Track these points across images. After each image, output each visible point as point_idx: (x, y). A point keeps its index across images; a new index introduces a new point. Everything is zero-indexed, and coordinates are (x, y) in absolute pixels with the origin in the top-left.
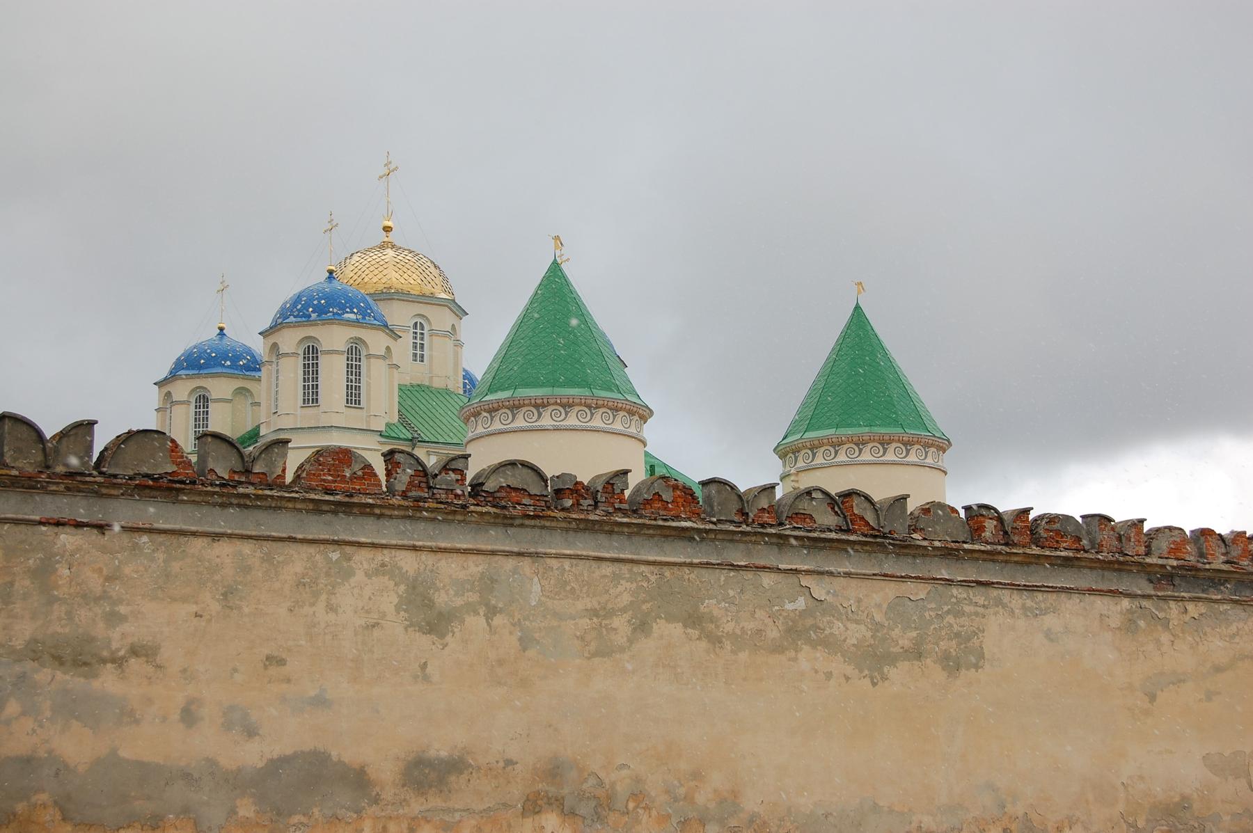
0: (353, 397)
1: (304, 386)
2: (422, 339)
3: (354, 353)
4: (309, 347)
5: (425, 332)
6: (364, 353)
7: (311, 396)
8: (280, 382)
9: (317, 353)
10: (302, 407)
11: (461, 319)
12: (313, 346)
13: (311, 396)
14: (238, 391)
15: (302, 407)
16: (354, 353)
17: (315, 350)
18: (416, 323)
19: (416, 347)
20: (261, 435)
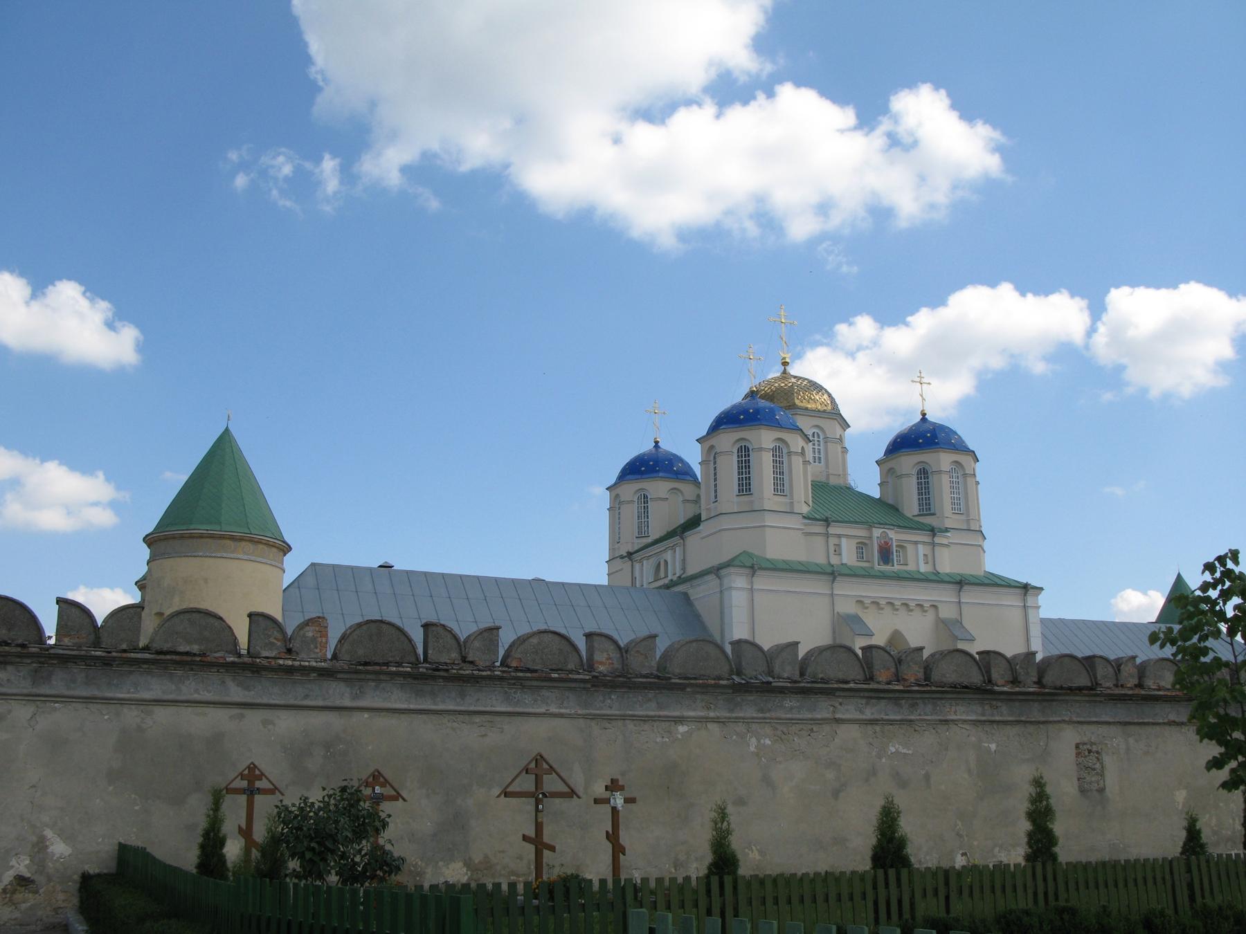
0: (780, 486)
1: (739, 478)
2: (819, 445)
3: (779, 453)
4: (741, 446)
5: (821, 439)
6: (785, 451)
7: (745, 486)
8: (718, 477)
9: (749, 451)
10: (737, 495)
11: (845, 430)
12: (745, 446)
13: (745, 486)
14: (672, 491)
15: (737, 495)
16: (779, 453)
17: (747, 449)
18: (814, 433)
19: (814, 452)
20: (702, 520)
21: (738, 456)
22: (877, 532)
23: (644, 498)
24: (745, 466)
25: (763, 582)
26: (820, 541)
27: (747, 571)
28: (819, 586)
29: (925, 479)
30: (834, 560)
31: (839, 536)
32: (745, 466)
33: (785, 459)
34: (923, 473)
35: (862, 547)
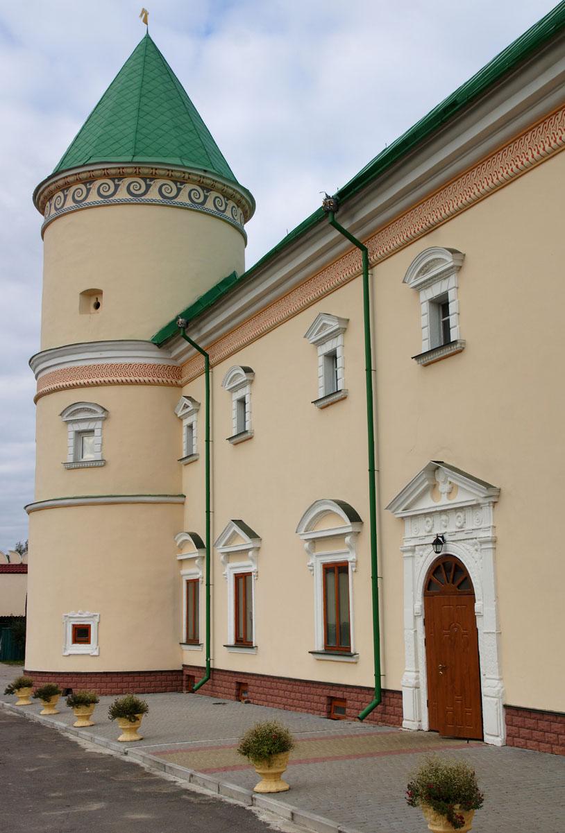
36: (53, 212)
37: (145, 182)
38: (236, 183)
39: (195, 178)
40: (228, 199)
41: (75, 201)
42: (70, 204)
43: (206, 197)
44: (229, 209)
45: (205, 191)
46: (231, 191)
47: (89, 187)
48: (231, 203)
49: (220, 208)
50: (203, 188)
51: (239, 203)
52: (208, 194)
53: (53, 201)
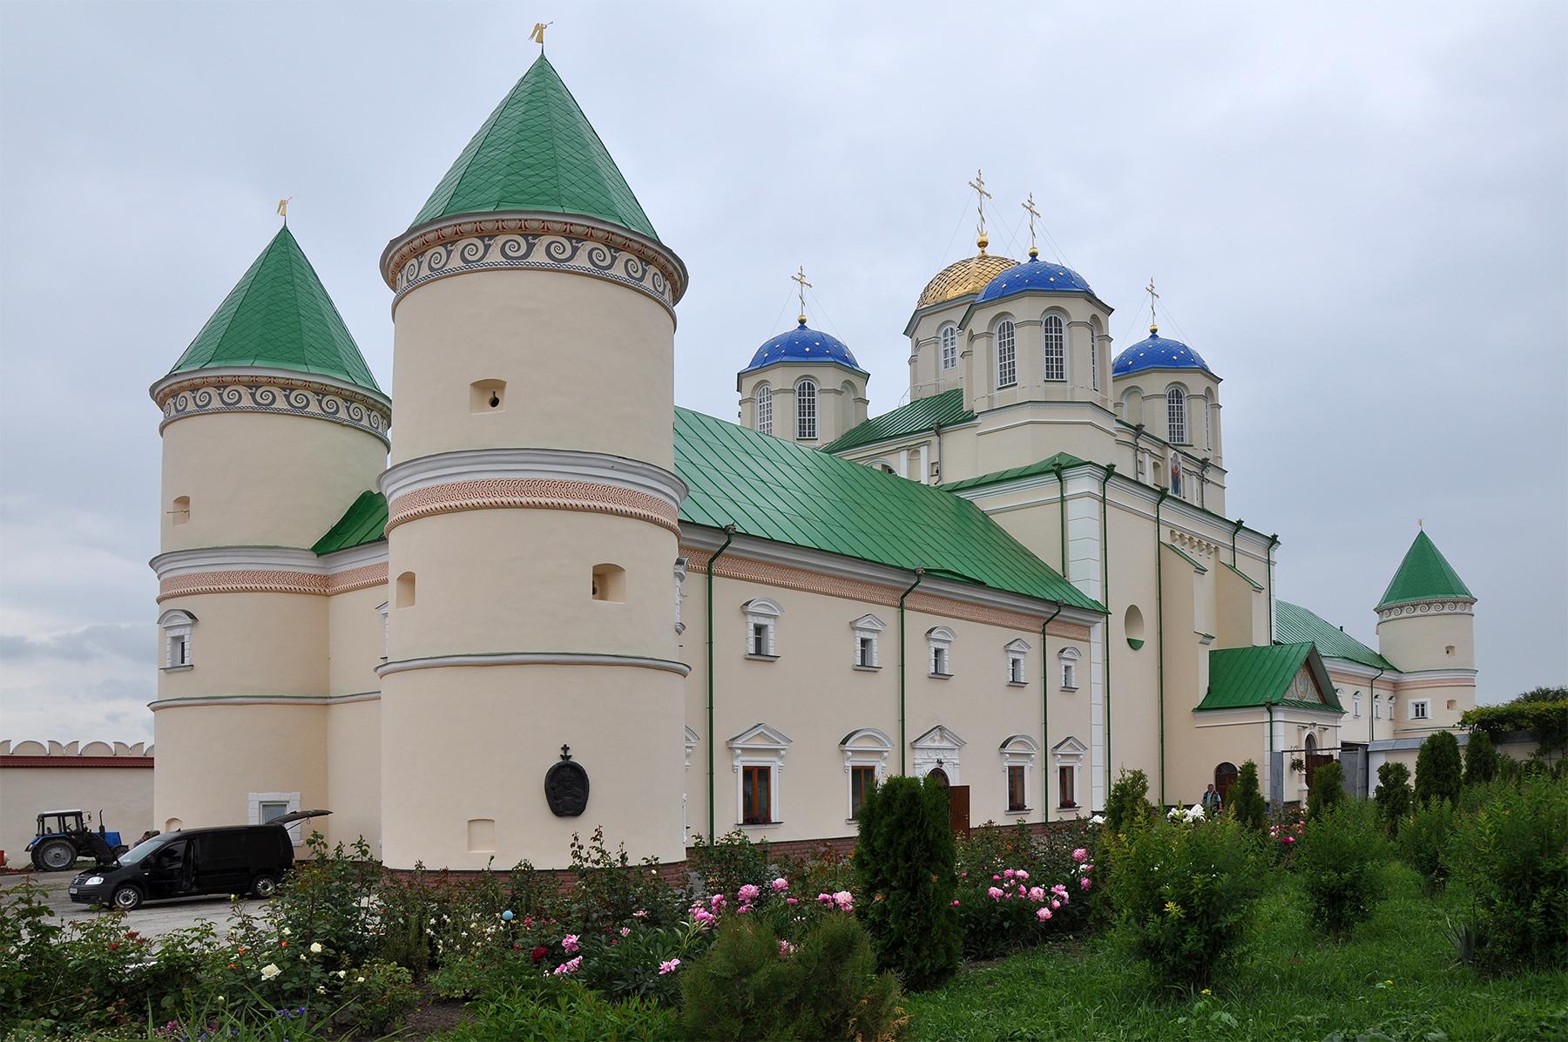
6: (1096, 334)
7: (1054, 371)
13: (1054, 371)
21: (1046, 329)
22: (1171, 453)
23: (809, 389)
24: (1054, 346)
25: (1115, 493)
26: (1129, 452)
27: (1101, 474)
28: (1145, 505)
29: (1177, 403)
30: (1141, 479)
31: (1144, 451)
32: (1054, 346)
33: (1096, 340)
34: (1176, 396)
35: (1156, 466)
36: (405, 284)
37: (527, 241)
38: (659, 244)
39: (600, 234)
40: (648, 263)
41: (431, 268)
42: (425, 272)
43: (614, 259)
44: (649, 277)
45: (612, 250)
46: (651, 253)
47: (449, 248)
48: (652, 270)
49: (633, 274)
50: (609, 247)
51: (663, 269)
52: (617, 255)
53: (404, 272)
